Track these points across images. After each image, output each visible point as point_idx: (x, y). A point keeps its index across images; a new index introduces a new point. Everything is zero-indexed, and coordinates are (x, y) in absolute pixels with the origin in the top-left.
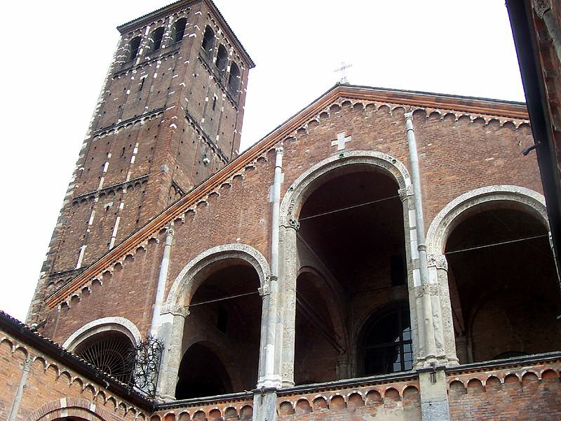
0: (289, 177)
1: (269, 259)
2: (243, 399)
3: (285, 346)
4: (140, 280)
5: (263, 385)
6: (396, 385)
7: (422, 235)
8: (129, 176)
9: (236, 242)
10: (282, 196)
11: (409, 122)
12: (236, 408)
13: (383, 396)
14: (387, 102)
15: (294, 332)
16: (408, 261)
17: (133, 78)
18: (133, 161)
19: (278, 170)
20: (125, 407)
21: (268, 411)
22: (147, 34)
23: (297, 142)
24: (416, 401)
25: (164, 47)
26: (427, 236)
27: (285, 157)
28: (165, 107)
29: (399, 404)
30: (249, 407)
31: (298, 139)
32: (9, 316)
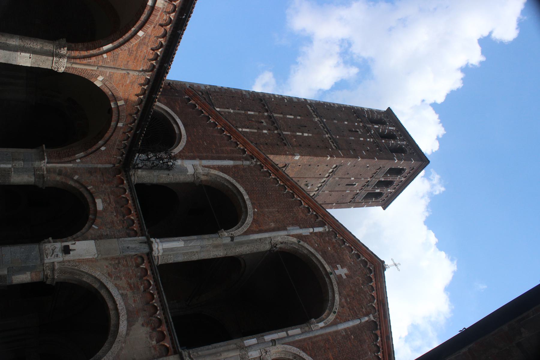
0: (308, 238)
1: (246, 233)
2: (141, 230)
3: (184, 254)
4: (214, 147)
5: (154, 242)
6: (168, 338)
7: (283, 341)
9: (254, 208)
10: (293, 236)
11: (366, 319)
12: (134, 225)
13: (158, 329)
14: (377, 300)
15: (196, 259)
16: (262, 334)
17: (356, 124)
18: (298, 134)
19: (311, 230)
20: (124, 148)
21: (135, 248)
22: (390, 128)
23: (334, 240)
24: (158, 355)
25: (383, 141)
26: (284, 345)
28: (341, 150)
29: (154, 342)
30: (136, 234)
31: (336, 241)
32: (174, 54)
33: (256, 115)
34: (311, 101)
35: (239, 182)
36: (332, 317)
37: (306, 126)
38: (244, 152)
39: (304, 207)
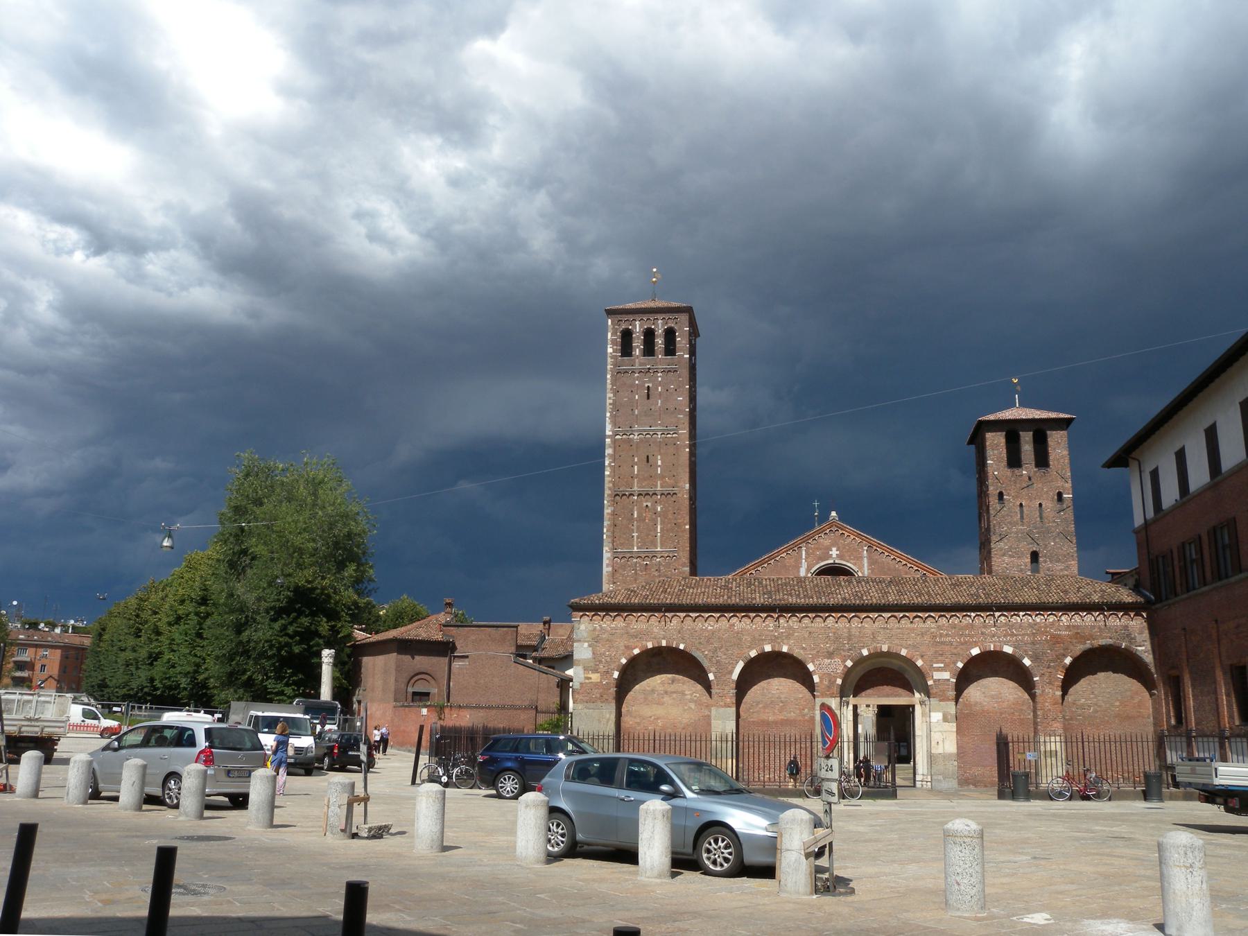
11: (865, 552)
17: (637, 382)
18: (659, 472)
19: (804, 561)
22: (638, 330)
25: (660, 356)
37: (648, 457)
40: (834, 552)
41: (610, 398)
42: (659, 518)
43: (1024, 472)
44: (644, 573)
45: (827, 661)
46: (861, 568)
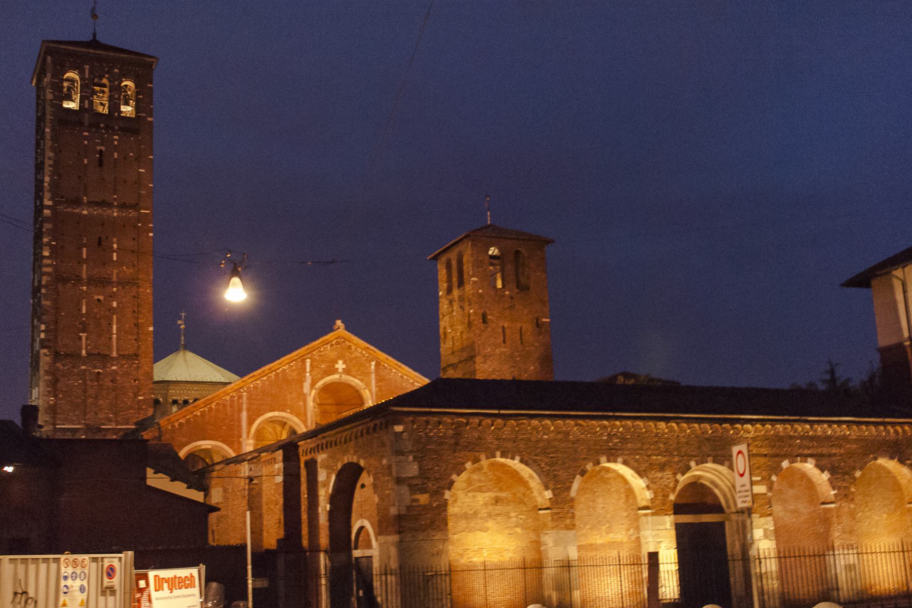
8: (115, 276)
9: (286, 412)
11: (373, 367)
18: (115, 259)
19: (308, 374)
27: (311, 365)
33: (87, 302)
34: (49, 198)
35: (263, 414)
36: (367, 391)
37: (100, 239)
38: (232, 397)
39: (288, 368)
40: (340, 365)
41: (50, 158)
42: (115, 317)
43: (507, 293)
44: (96, 383)
45: (659, 475)
46: (368, 385)
